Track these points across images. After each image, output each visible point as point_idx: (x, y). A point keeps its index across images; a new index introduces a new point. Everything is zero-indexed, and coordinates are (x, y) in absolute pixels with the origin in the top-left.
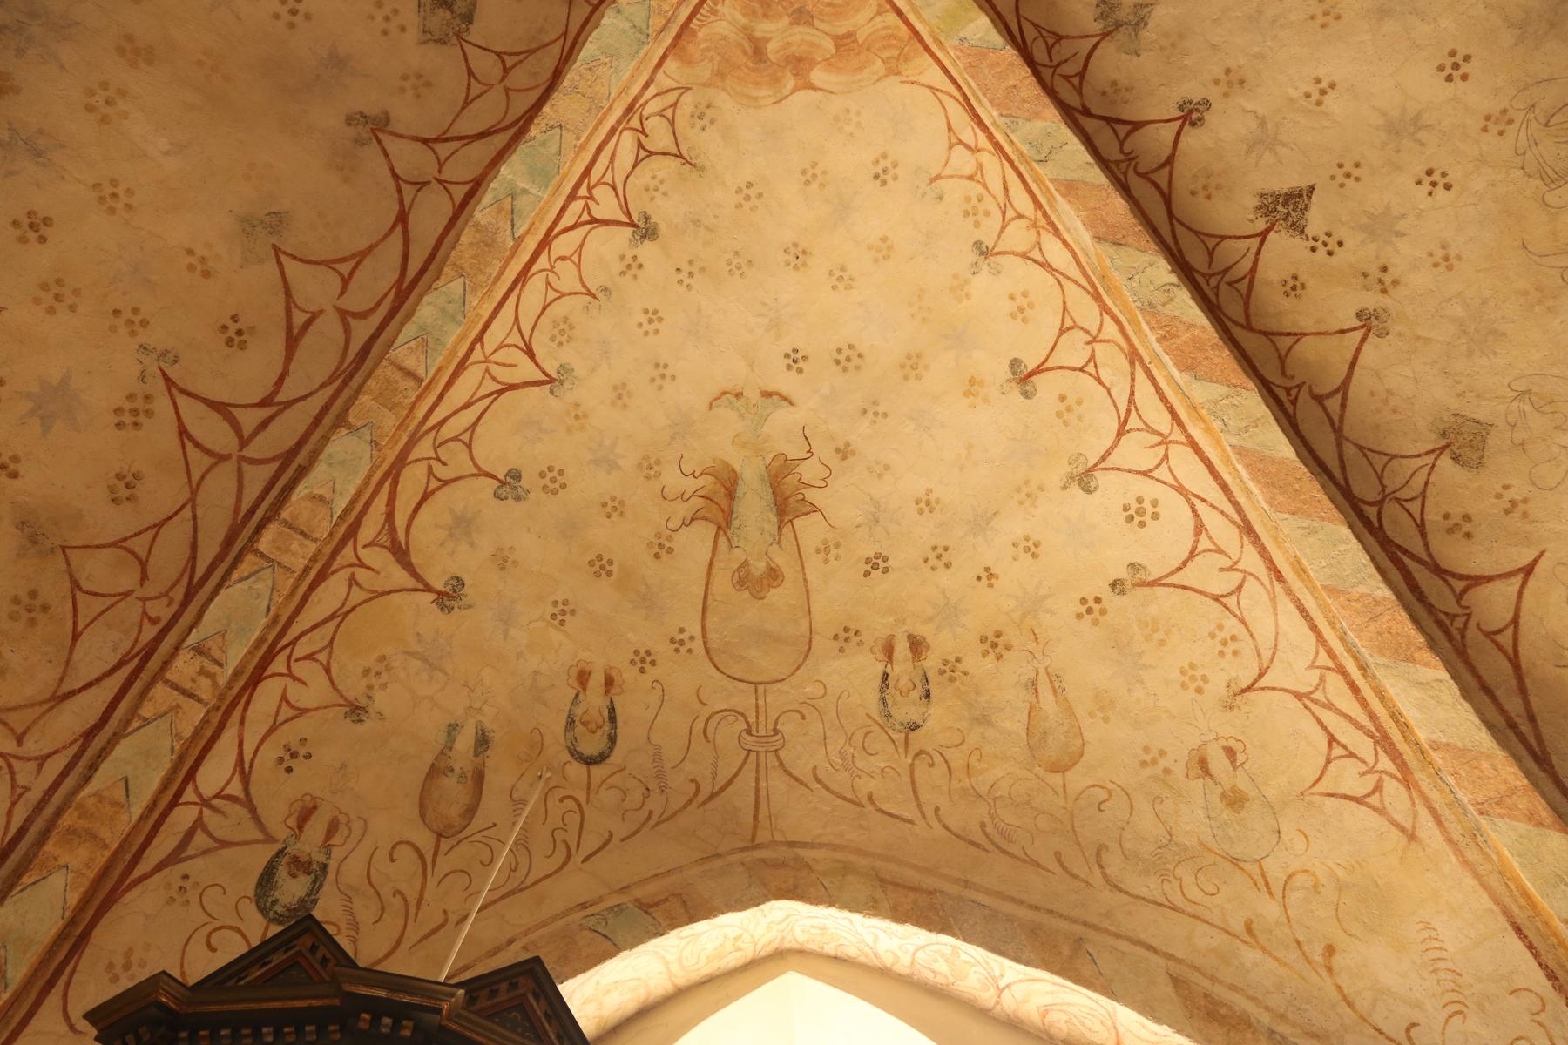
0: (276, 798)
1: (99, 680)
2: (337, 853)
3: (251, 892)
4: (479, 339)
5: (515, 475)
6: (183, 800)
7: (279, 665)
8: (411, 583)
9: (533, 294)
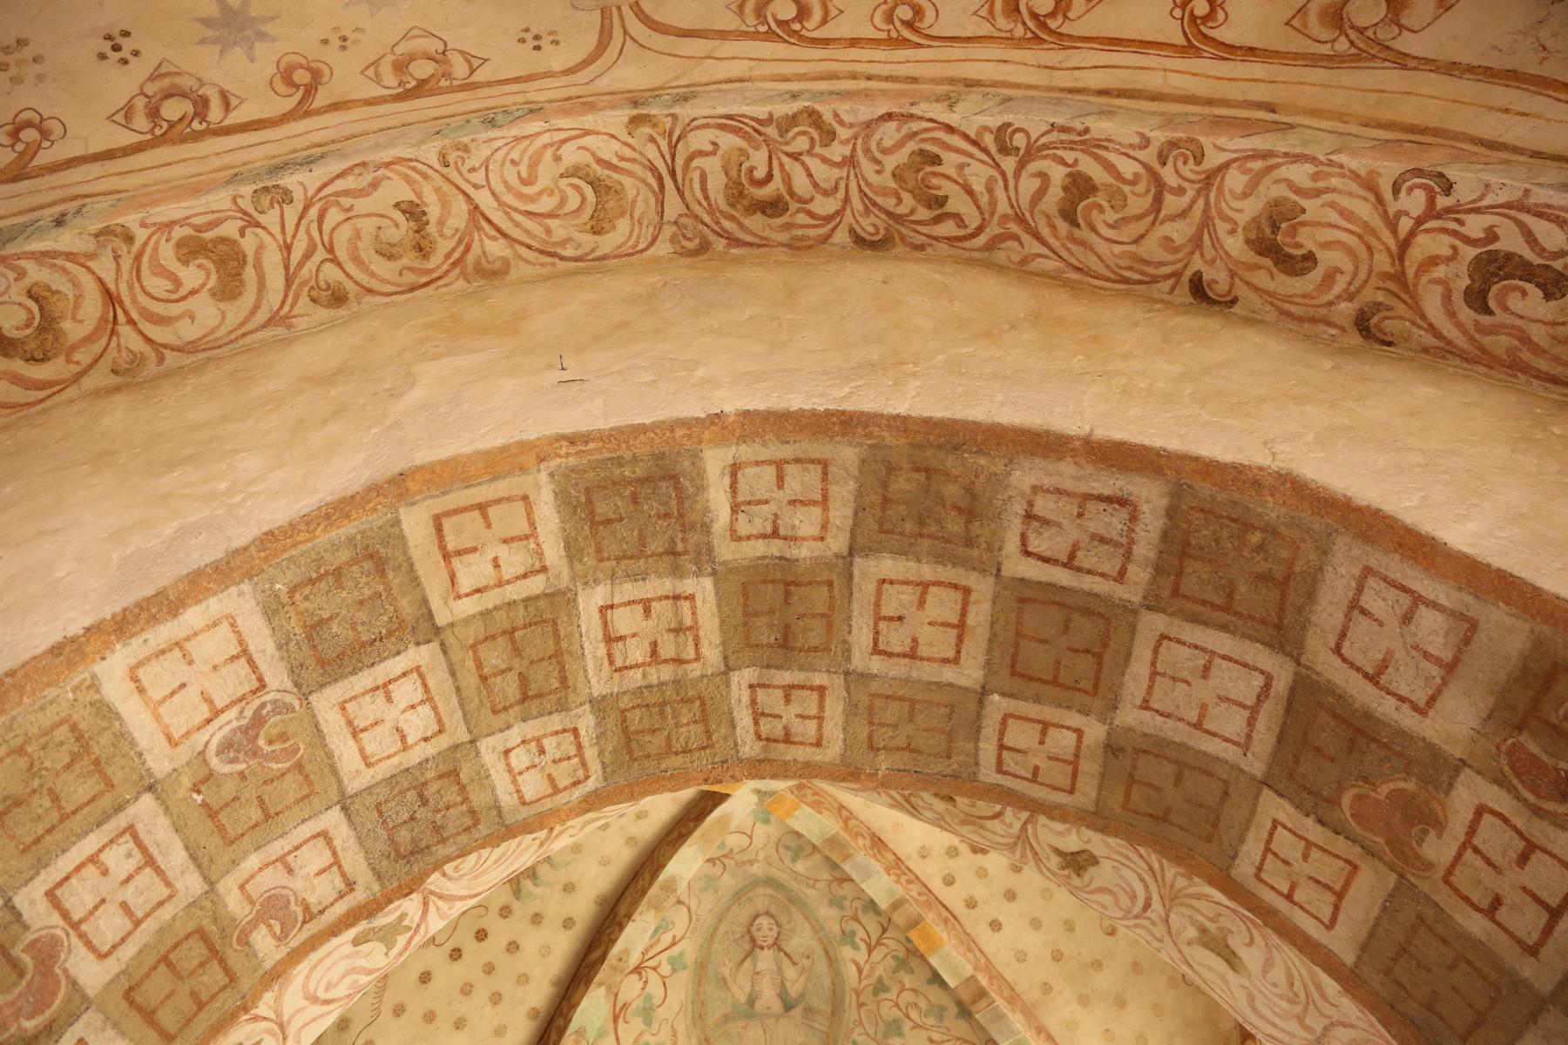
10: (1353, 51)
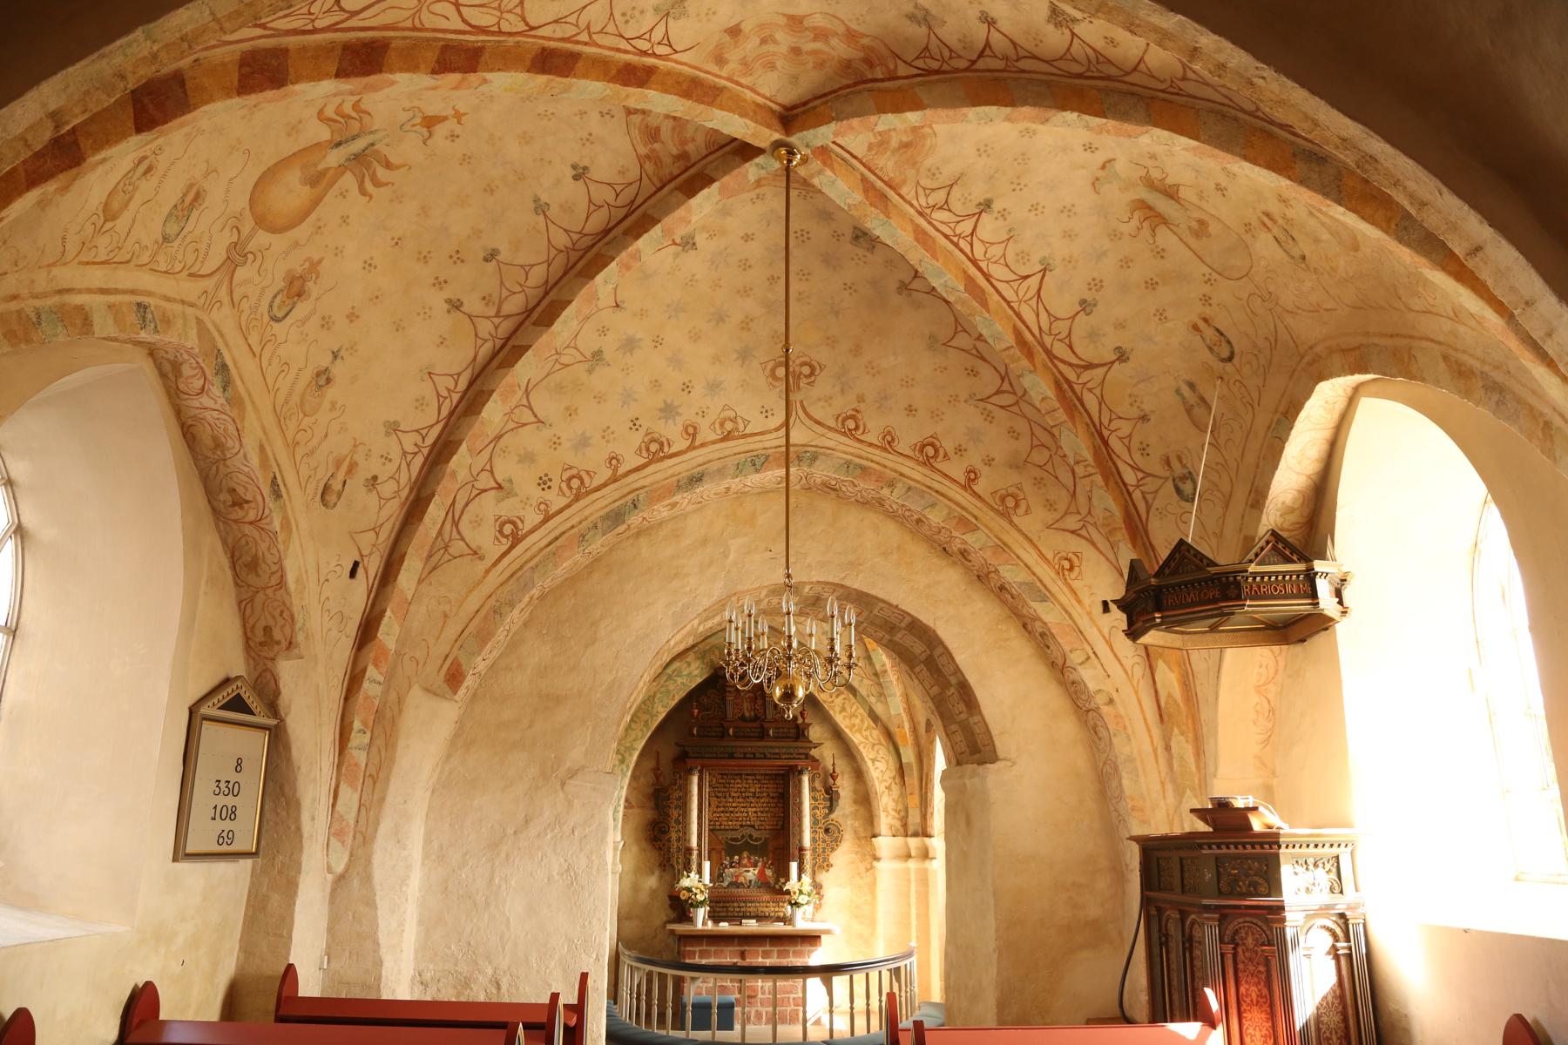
0: (1155, 466)
4: (1008, 303)
5: (1083, 302)
7: (1106, 433)
8: (1105, 369)
9: (998, 271)
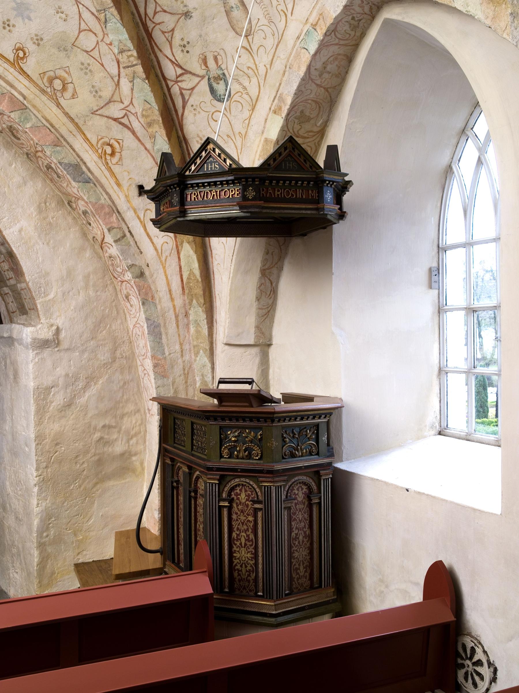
1: (119, 71)
2: (223, 67)
3: (212, 98)
6: (170, 86)
7: (150, 25)
10: (50, 93)
